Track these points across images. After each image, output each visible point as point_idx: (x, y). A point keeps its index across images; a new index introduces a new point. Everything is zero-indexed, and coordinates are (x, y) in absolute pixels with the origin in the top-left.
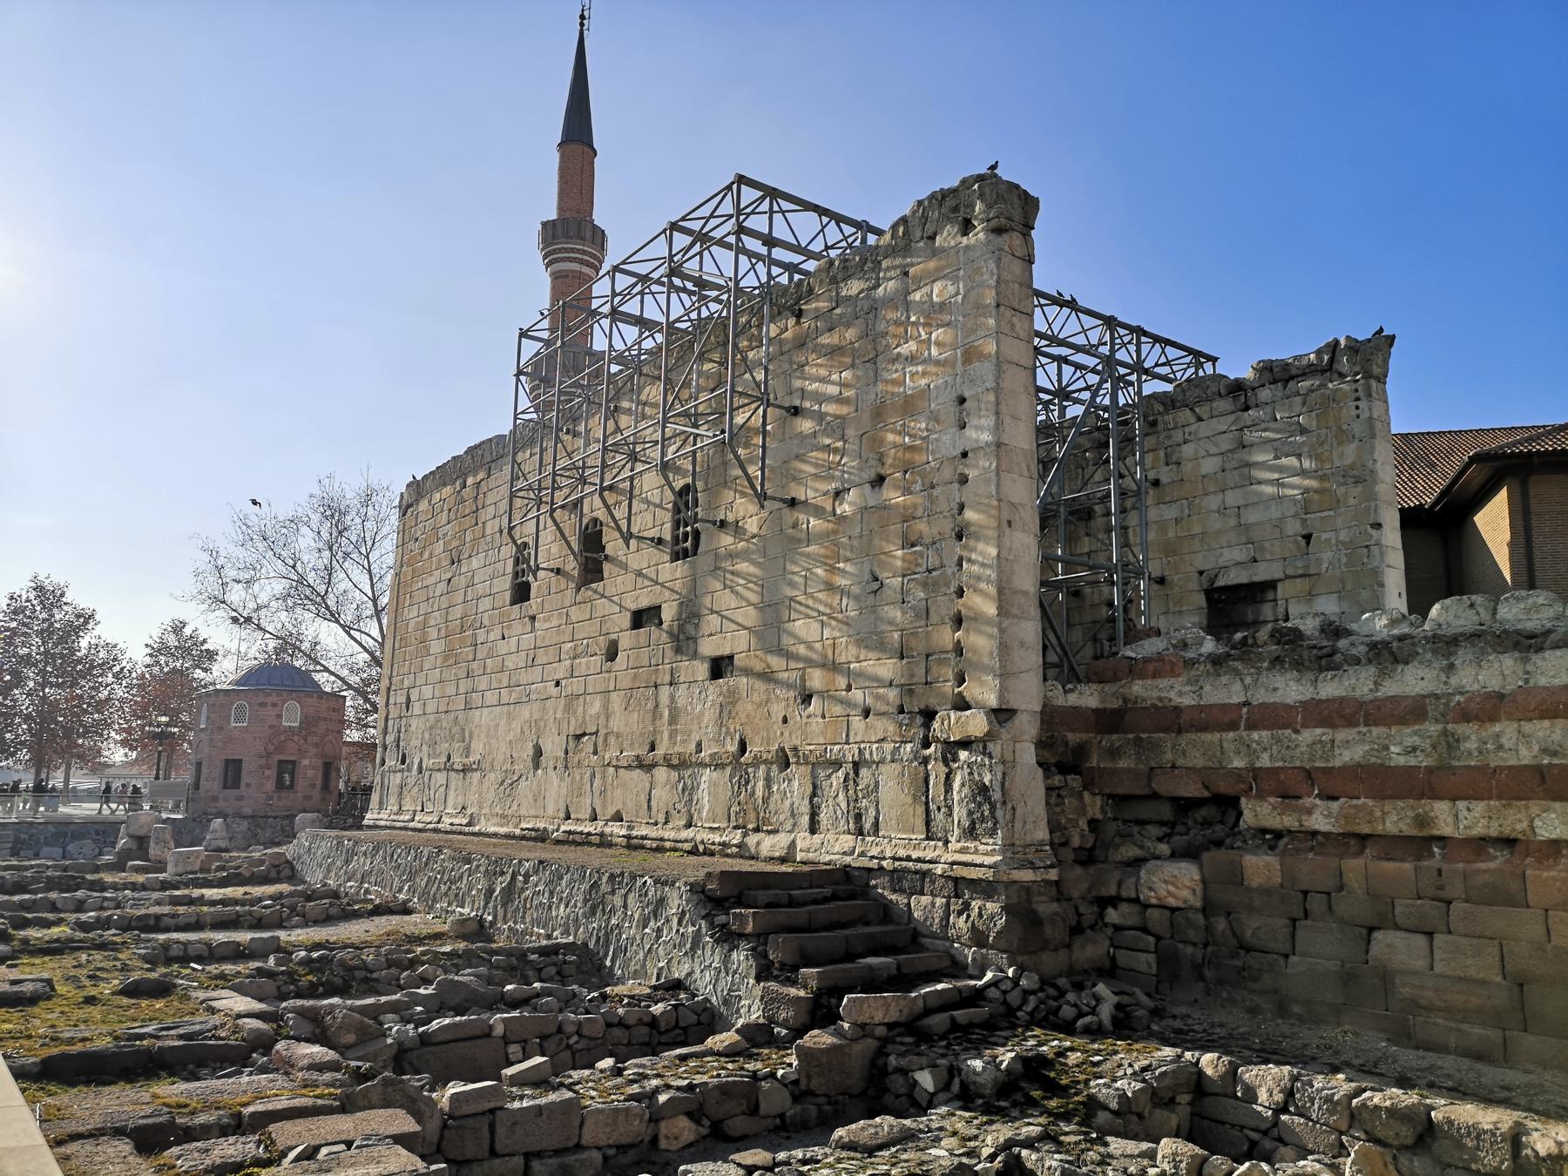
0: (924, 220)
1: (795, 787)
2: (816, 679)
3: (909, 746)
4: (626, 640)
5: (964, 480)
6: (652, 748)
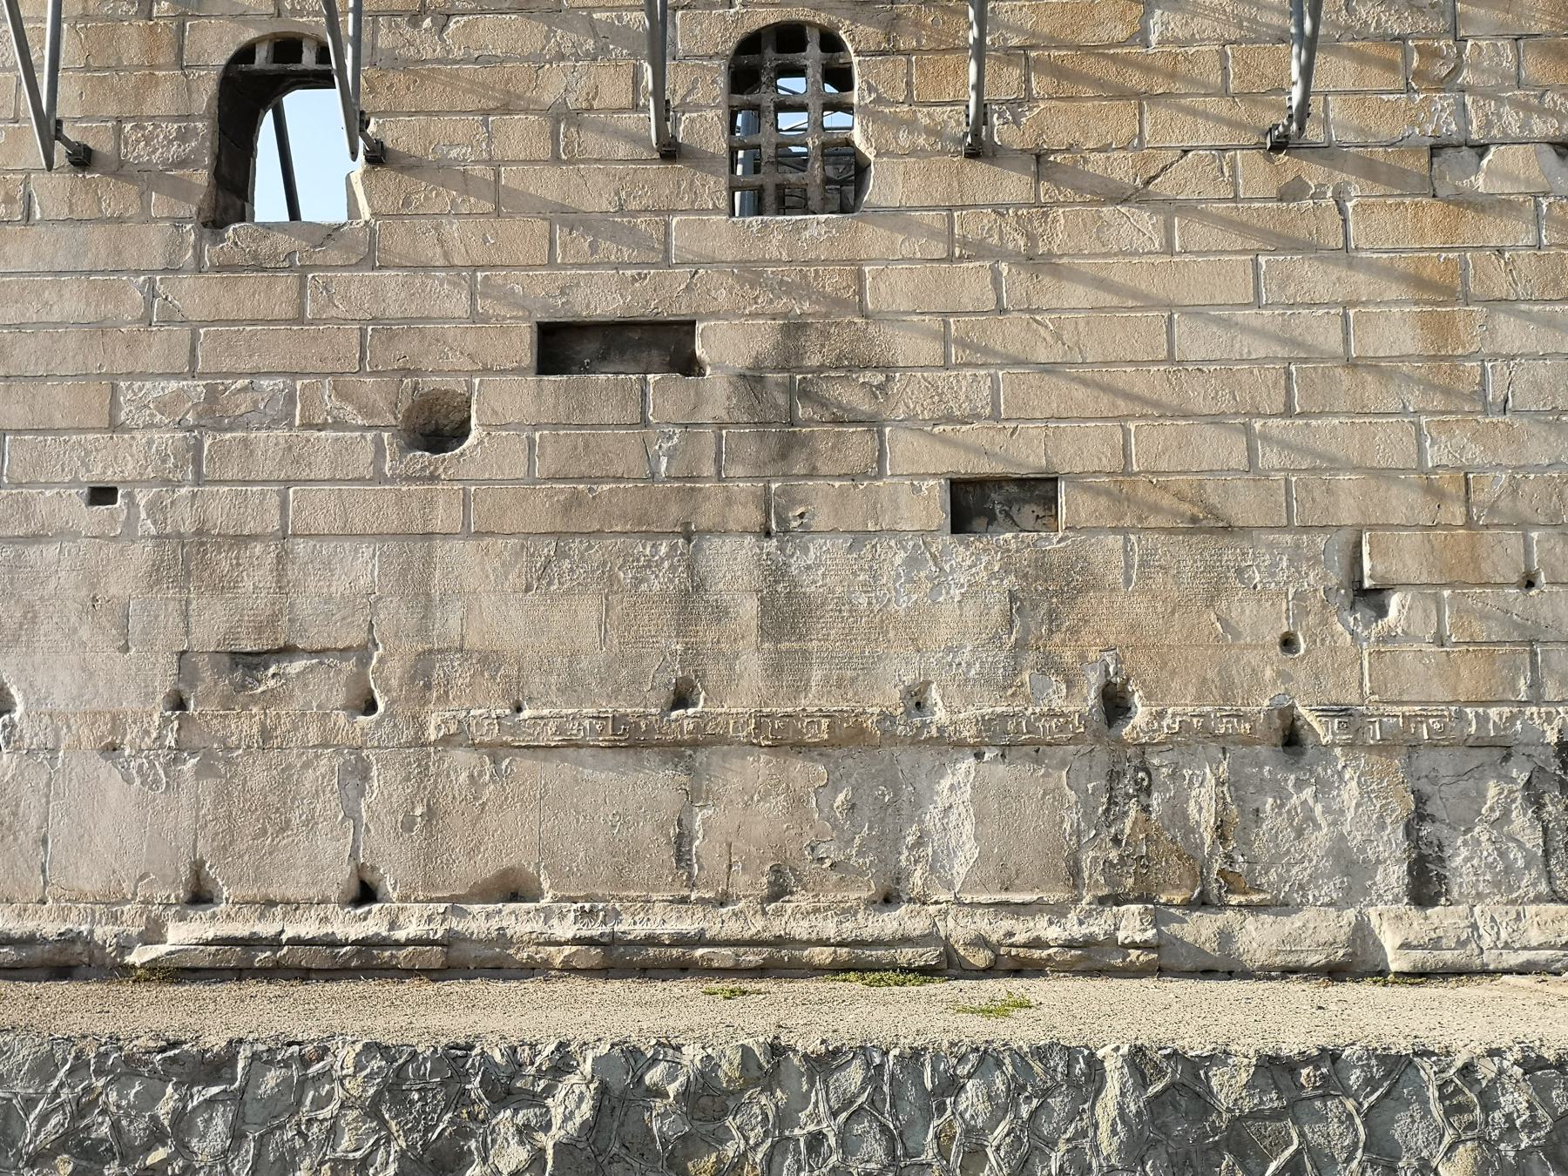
1: (1353, 804)
4: (510, 404)
6: (681, 699)
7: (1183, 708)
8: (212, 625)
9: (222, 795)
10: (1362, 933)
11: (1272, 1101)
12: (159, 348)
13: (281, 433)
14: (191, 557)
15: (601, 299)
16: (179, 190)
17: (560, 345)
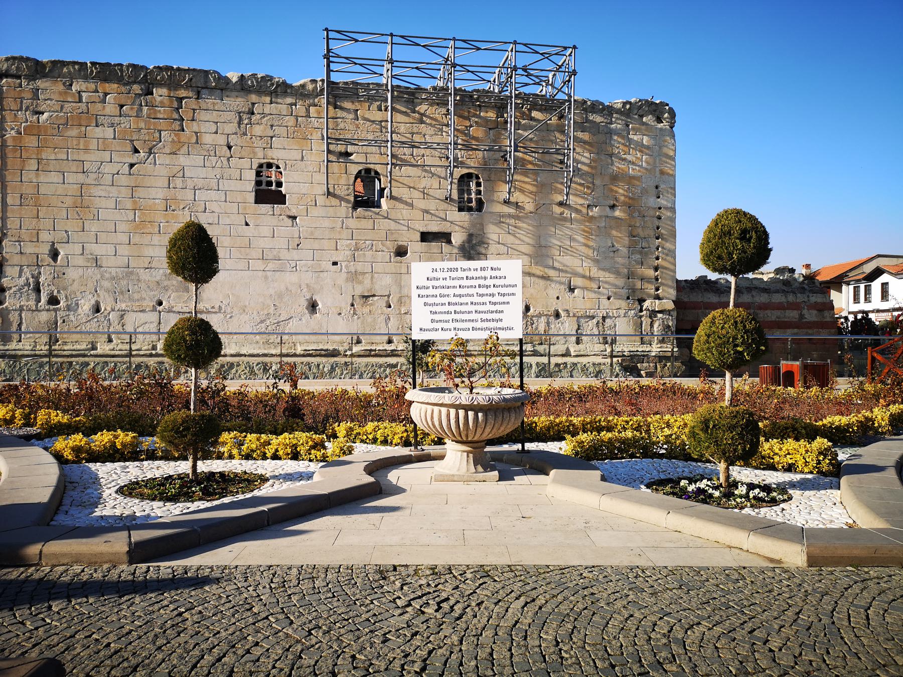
0: (640, 107)
2: (577, 281)
3: (633, 312)
5: (659, 218)
7: (539, 310)
8: (359, 290)
9: (363, 323)
10: (568, 349)
11: (557, 369)
12: (346, 234)
13: (371, 252)
14: (354, 276)
15: (434, 228)
16: (348, 201)
17: (426, 237)
